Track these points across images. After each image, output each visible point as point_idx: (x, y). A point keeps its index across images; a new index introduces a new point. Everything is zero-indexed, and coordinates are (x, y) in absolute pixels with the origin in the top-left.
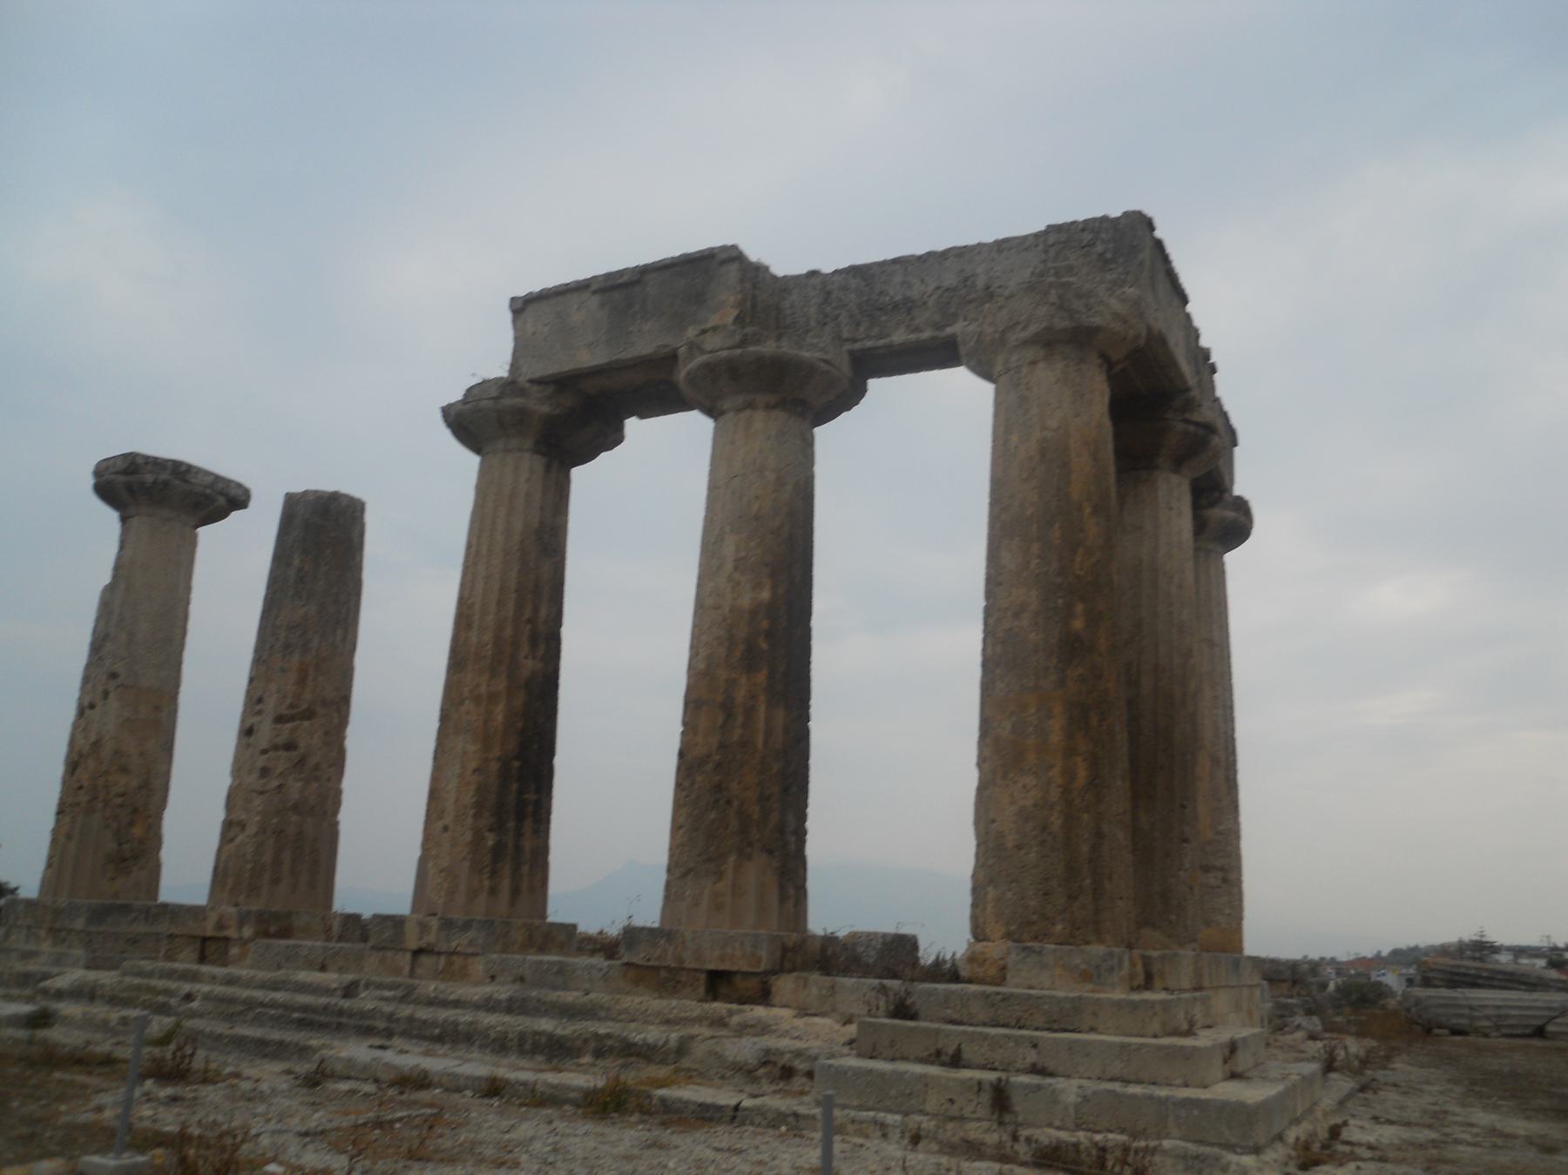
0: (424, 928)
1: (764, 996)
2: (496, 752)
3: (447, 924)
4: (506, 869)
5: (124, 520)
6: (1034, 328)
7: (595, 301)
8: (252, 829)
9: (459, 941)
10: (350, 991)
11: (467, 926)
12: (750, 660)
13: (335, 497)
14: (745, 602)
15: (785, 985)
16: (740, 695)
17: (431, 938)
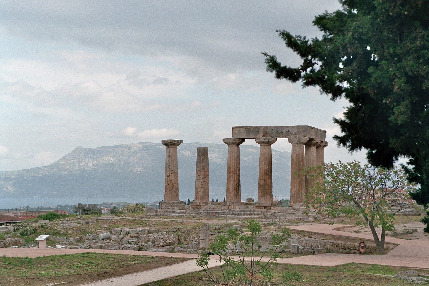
0: (230, 203)
1: (270, 209)
2: (236, 183)
3: (233, 203)
4: (238, 196)
5: (168, 148)
6: (296, 142)
7: (244, 129)
8: (202, 192)
9: (235, 205)
10: (222, 210)
11: (235, 203)
12: (266, 175)
13: (205, 148)
14: (266, 168)
15: (272, 208)
16: (266, 178)
17: (231, 204)
